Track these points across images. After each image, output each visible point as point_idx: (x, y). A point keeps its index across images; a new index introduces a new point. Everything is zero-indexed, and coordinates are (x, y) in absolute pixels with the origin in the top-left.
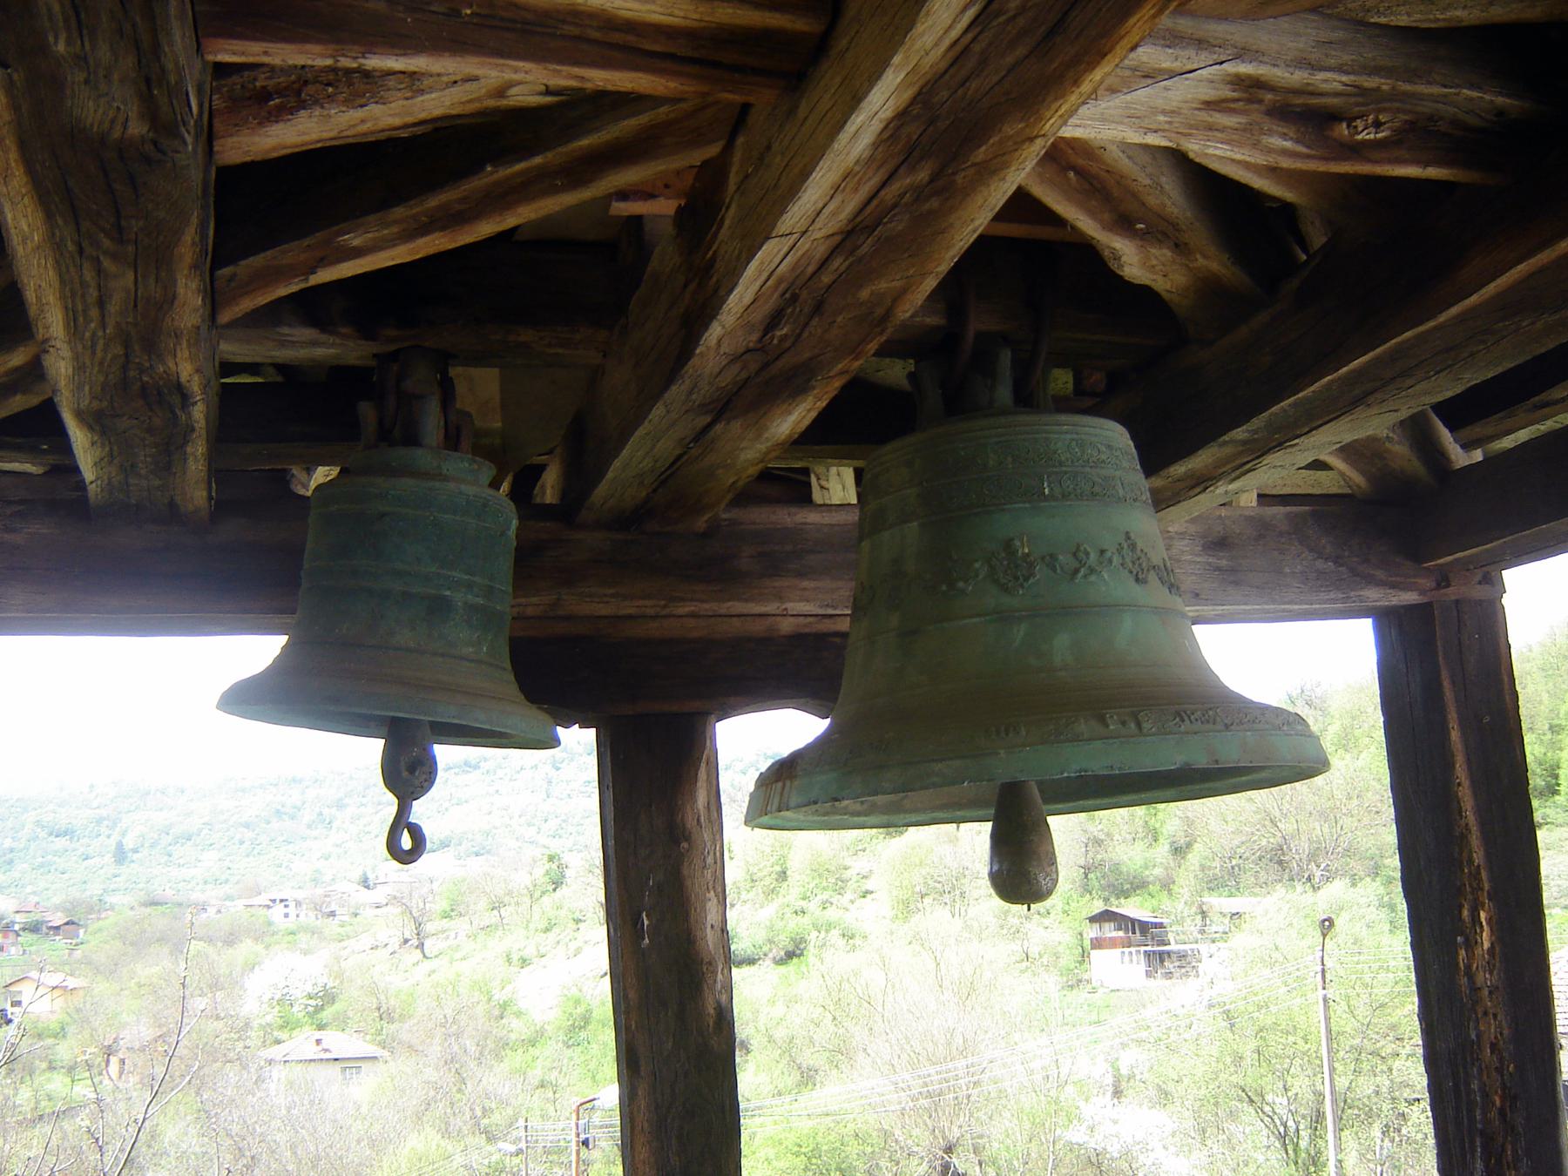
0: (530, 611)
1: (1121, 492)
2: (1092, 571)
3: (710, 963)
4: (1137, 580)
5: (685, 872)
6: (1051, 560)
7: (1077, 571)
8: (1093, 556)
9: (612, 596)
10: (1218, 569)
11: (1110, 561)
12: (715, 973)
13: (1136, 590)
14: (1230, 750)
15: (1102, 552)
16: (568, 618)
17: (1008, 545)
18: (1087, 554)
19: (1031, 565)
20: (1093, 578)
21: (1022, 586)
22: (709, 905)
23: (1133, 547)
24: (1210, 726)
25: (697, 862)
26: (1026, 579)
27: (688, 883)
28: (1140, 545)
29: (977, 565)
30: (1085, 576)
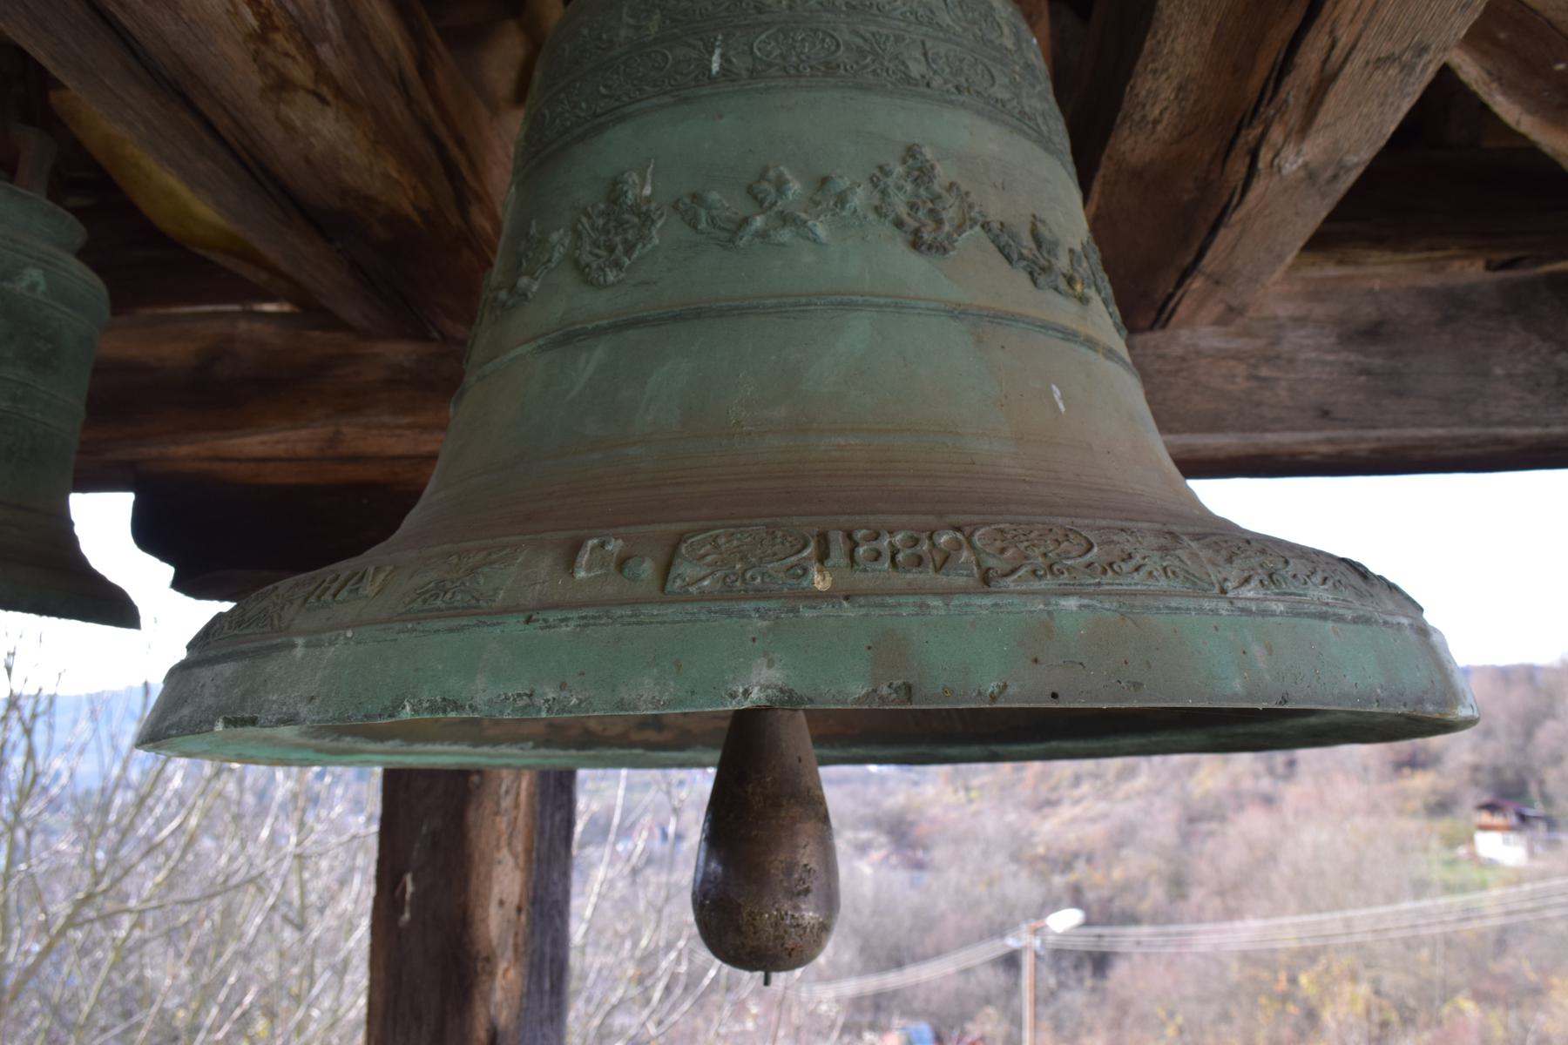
0: (301, 449)
1: (916, 69)
2: (786, 219)
3: (487, 959)
4: (916, 243)
5: (471, 816)
6: (690, 208)
7: (746, 221)
8: (795, 187)
9: (410, 427)
10: (1366, 371)
11: (842, 199)
12: (492, 975)
13: (914, 270)
14: (1350, 672)
15: (824, 181)
16: (356, 459)
17: (614, 191)
18: (781, 186)
19: (647, 219)
20: (786, 235)
21: (617, 265)
22: (498, 871)
23: (922, 173)
24: (927, 576)
25: (489, 805)
26: (629, 248)
27: (473, 834)
28: (944, 173)
29: (555, 237)
30: (763, 235)
